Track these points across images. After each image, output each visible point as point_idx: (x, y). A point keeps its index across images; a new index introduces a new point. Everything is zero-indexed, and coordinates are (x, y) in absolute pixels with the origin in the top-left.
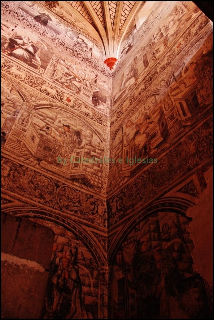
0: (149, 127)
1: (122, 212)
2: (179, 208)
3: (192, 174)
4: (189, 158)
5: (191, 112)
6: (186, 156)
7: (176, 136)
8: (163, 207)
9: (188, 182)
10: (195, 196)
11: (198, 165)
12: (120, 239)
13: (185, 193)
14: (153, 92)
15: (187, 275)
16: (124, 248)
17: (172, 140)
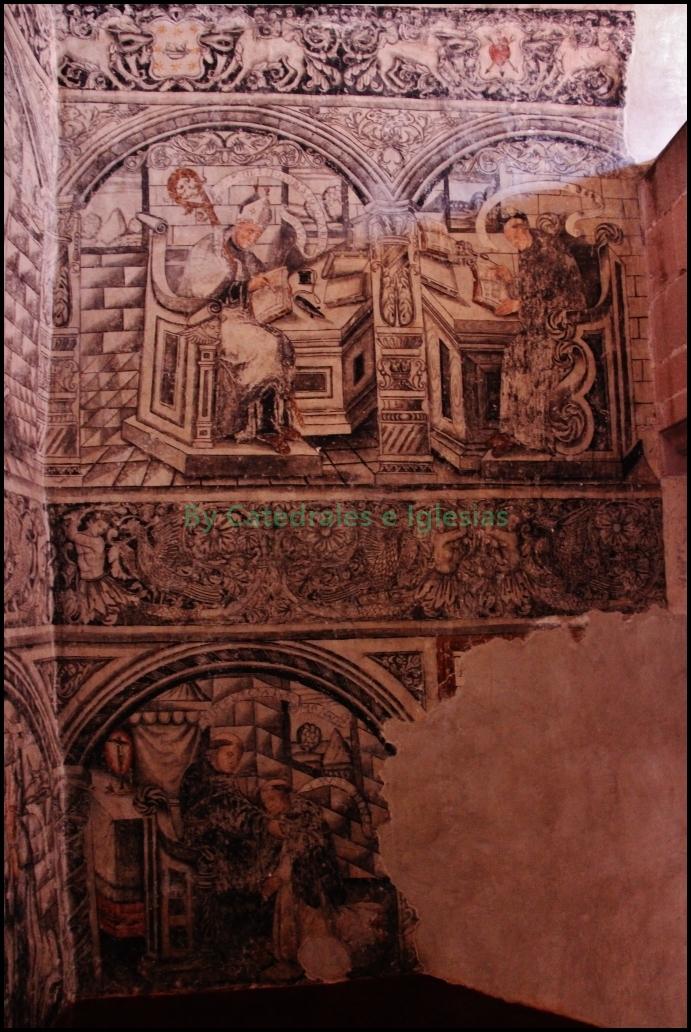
0: (296, 318)
1: (135, 599)
2: (364, 704)
3: (424, 634)
4: (427, 579)
5: (468, 420)
6: (416, 562)
7: (402, 470)
8: (312, 673)
9: (407, 648)
10: (417, 699)
11: (447, 618)
12: (127, 693)
13: (390, 672)
14: (339, 152)
15: (358, 872)
16: (140, 729)
17: (385, 470)
